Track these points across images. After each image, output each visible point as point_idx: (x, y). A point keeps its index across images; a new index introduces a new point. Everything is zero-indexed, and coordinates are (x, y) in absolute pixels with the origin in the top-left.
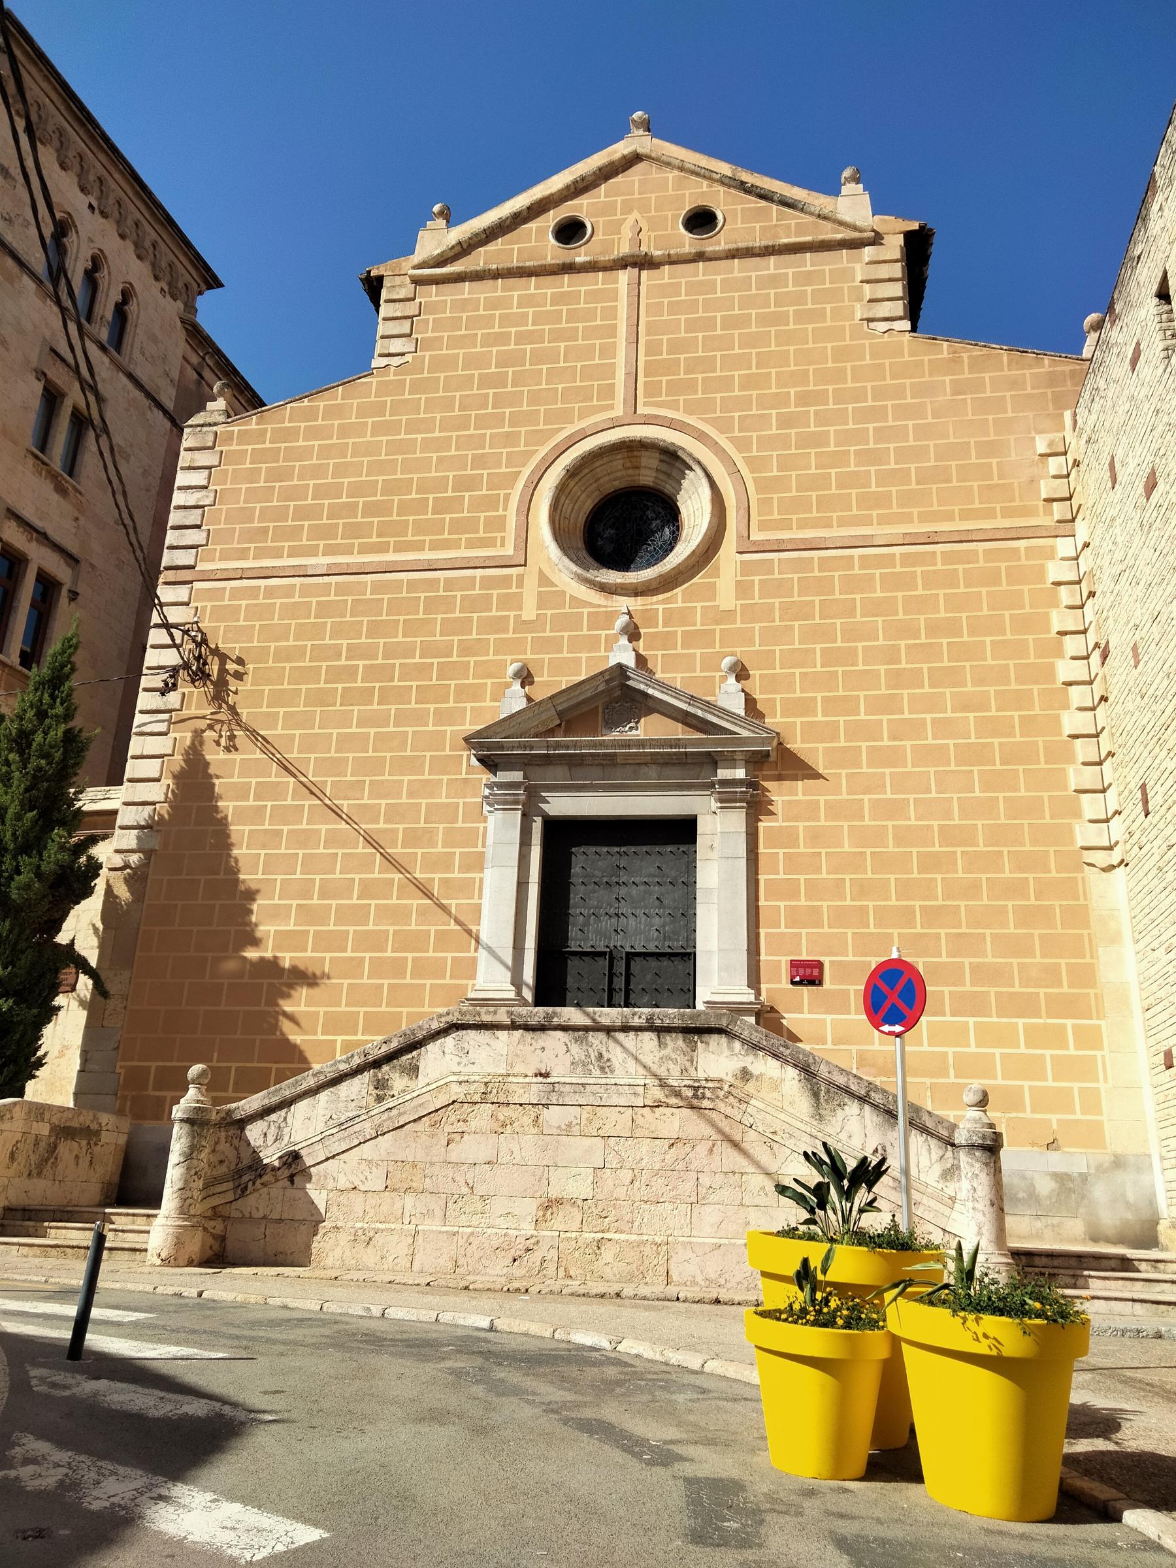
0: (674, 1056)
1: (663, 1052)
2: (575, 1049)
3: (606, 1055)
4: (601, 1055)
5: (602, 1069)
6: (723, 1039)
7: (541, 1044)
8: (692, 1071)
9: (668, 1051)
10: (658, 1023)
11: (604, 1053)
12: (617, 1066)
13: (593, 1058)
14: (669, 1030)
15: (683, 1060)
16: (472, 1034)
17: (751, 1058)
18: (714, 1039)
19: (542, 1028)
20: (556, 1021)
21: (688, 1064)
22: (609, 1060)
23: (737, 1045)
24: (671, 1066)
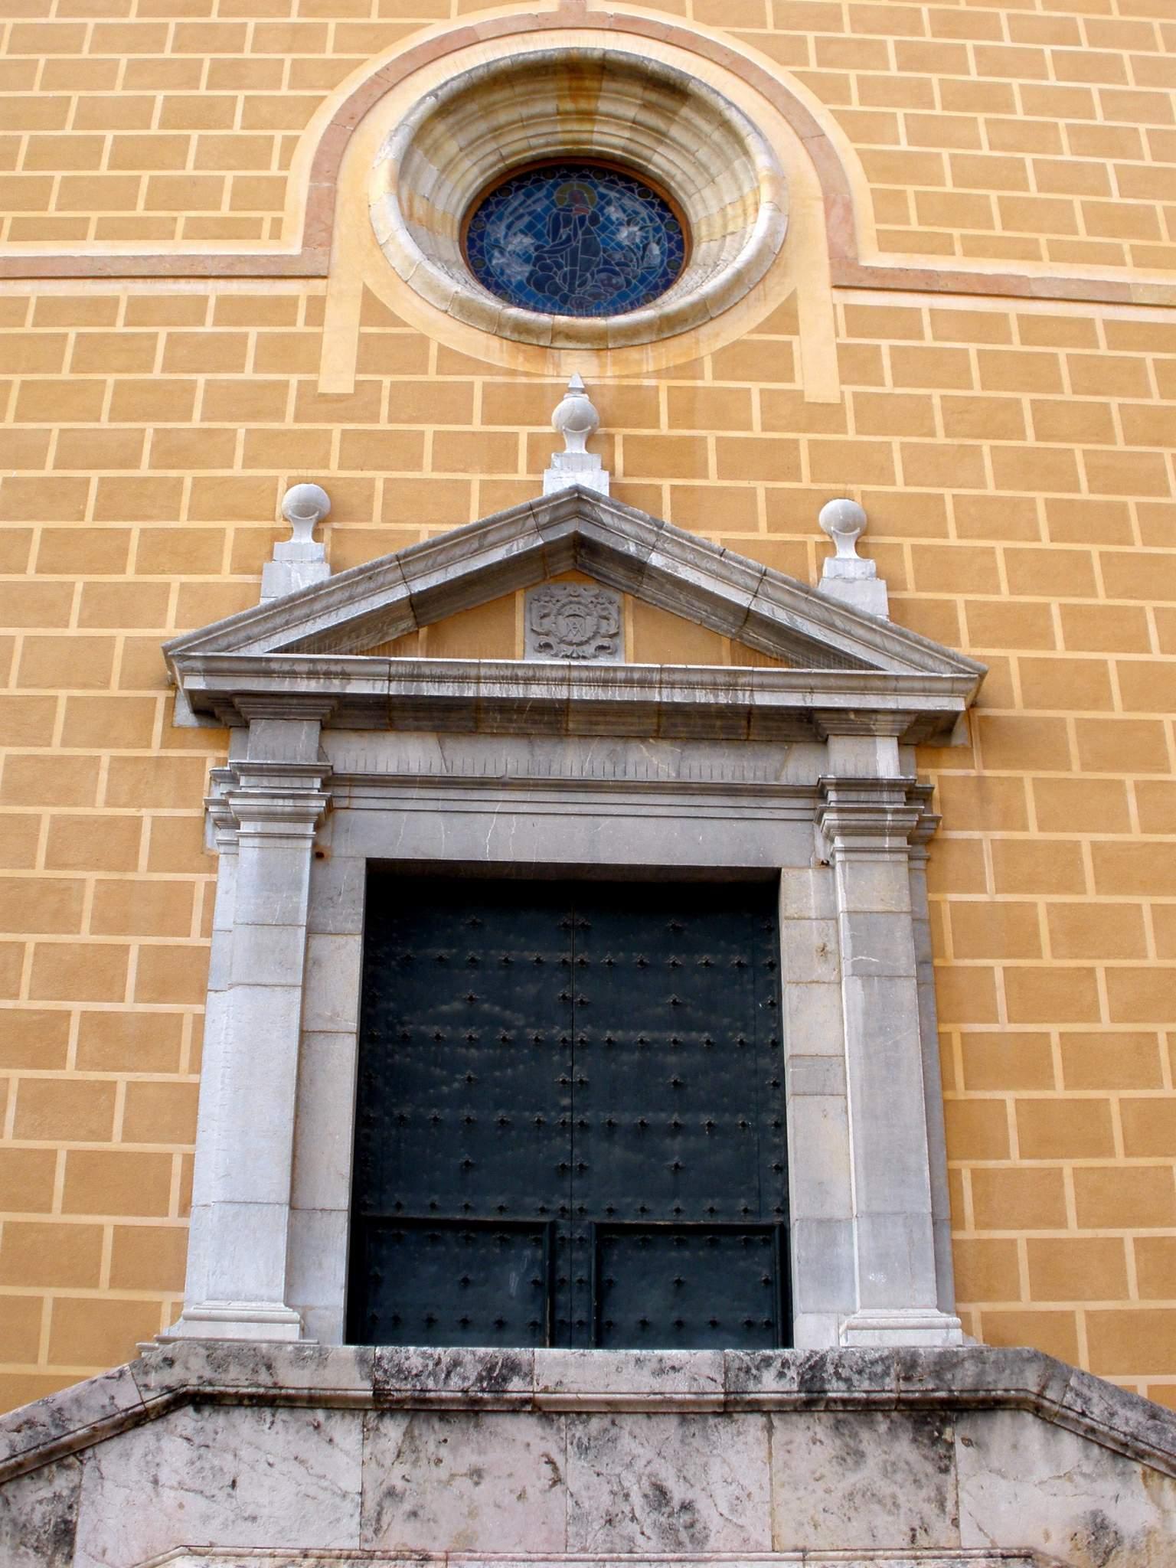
0: (885, 1488)
1: (855, 1479)
2: (576, 1471)
3: (678, 1493)
4: (660, 1495)
5: (668, 1532)
6: (1032, 1431)
7: (469, 1457)
8: (942, 1531)
9: (869, 1472)
10: (836, 1390)
11: (672, 1484)
12: (715, 1523)
13: (637, 1499)
14: (867, 1408)
15: (915, 1501)
16: (244, 1423)
17: (1109, 1486)
18: (1002, 1428)
19: (472, 1410)
20: (516, 1386)
21: (930, 1510)
22: (686, 1507)
23: (1069, 1446)
24: (882, 1520)
